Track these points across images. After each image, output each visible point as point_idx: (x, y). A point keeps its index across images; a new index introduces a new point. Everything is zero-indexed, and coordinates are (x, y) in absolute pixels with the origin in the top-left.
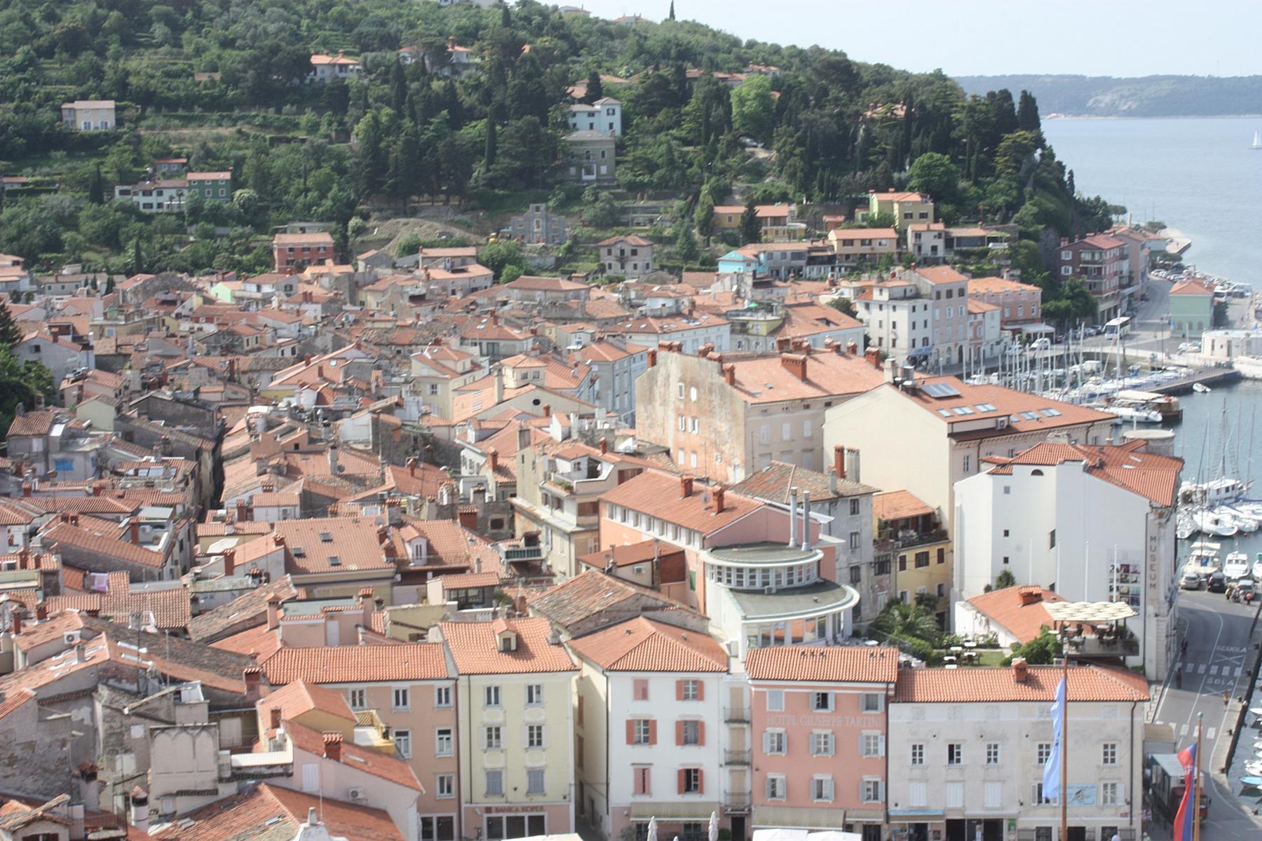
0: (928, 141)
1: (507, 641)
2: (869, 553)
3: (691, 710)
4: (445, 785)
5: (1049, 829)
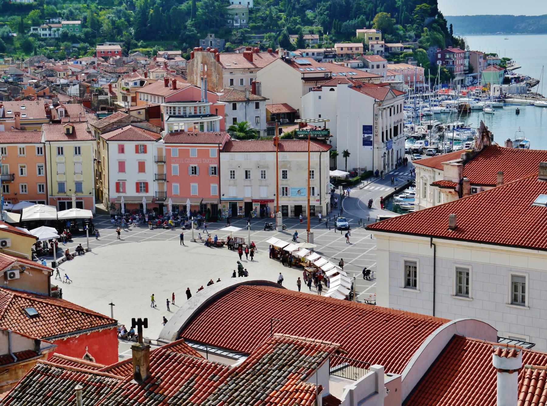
0: (383, 9)
1: (68, 130)
3: (141, 157)
4: (41, 187)
5: (287, 206)
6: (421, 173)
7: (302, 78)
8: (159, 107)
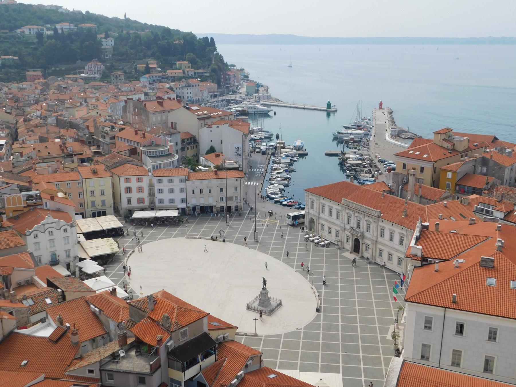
2: (180, 146)
3: (140, 184)
4: (81, 205)
6: (310, 196)
7: (197, 119)
8: (136, 148)
